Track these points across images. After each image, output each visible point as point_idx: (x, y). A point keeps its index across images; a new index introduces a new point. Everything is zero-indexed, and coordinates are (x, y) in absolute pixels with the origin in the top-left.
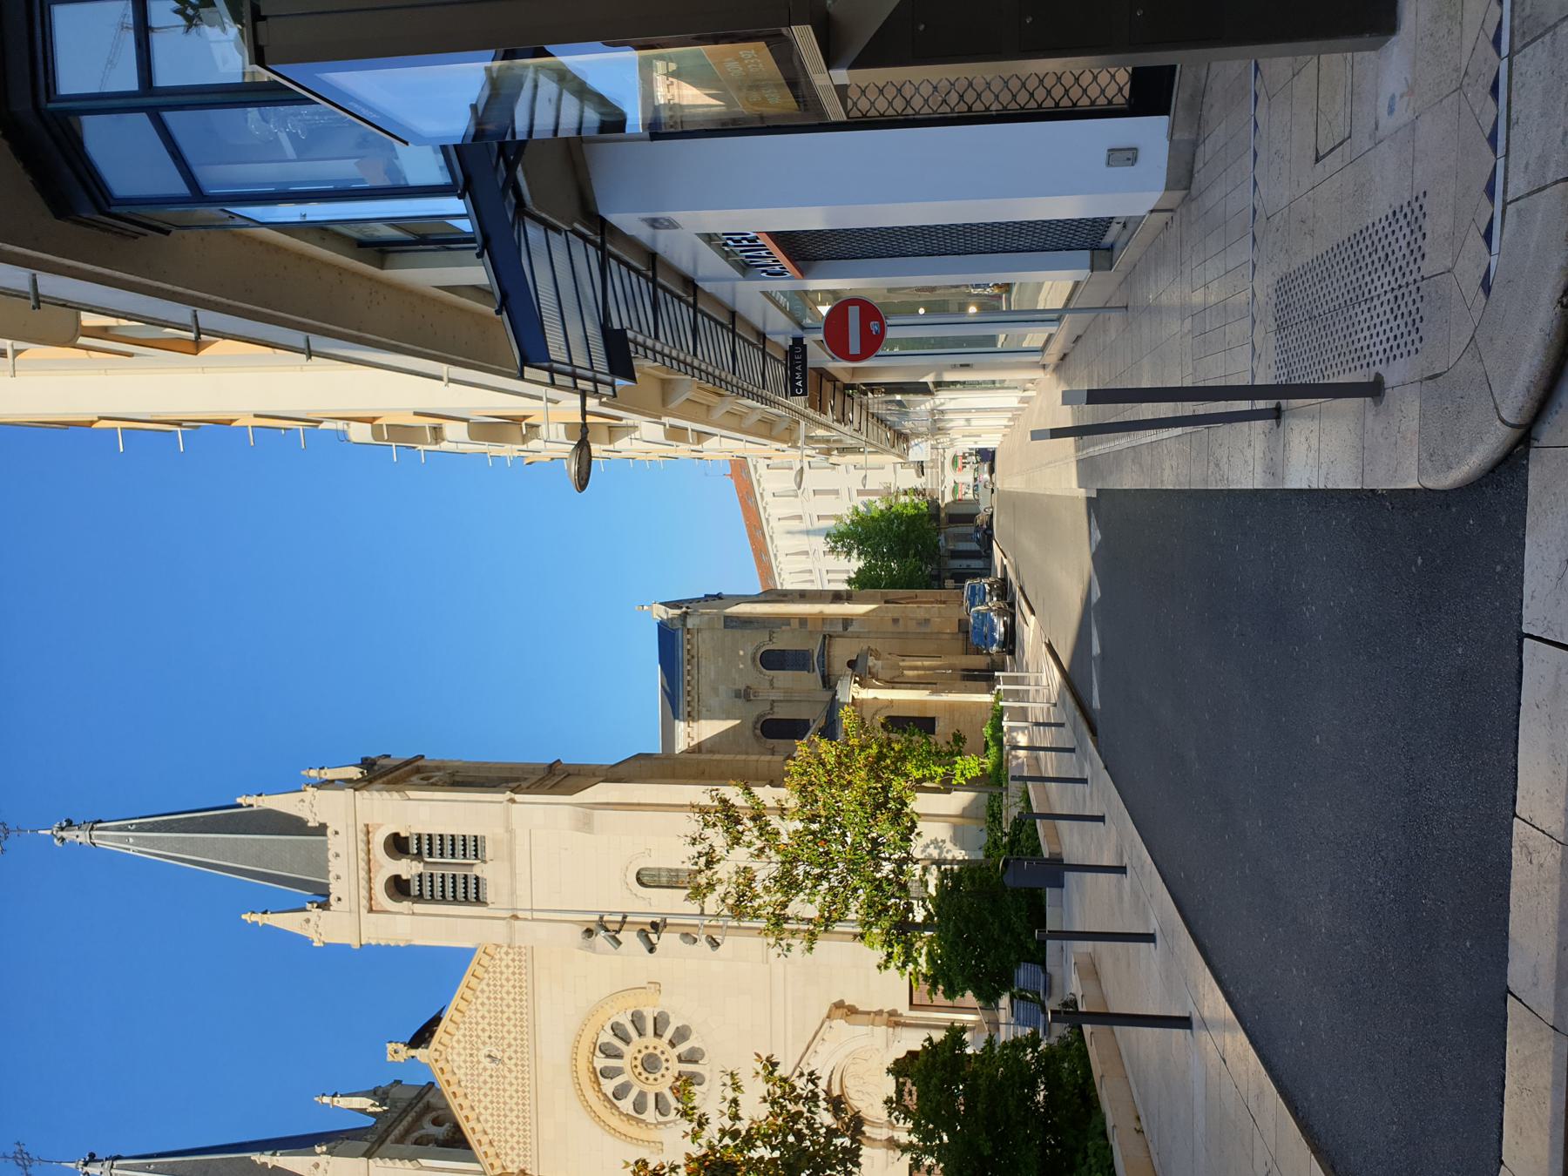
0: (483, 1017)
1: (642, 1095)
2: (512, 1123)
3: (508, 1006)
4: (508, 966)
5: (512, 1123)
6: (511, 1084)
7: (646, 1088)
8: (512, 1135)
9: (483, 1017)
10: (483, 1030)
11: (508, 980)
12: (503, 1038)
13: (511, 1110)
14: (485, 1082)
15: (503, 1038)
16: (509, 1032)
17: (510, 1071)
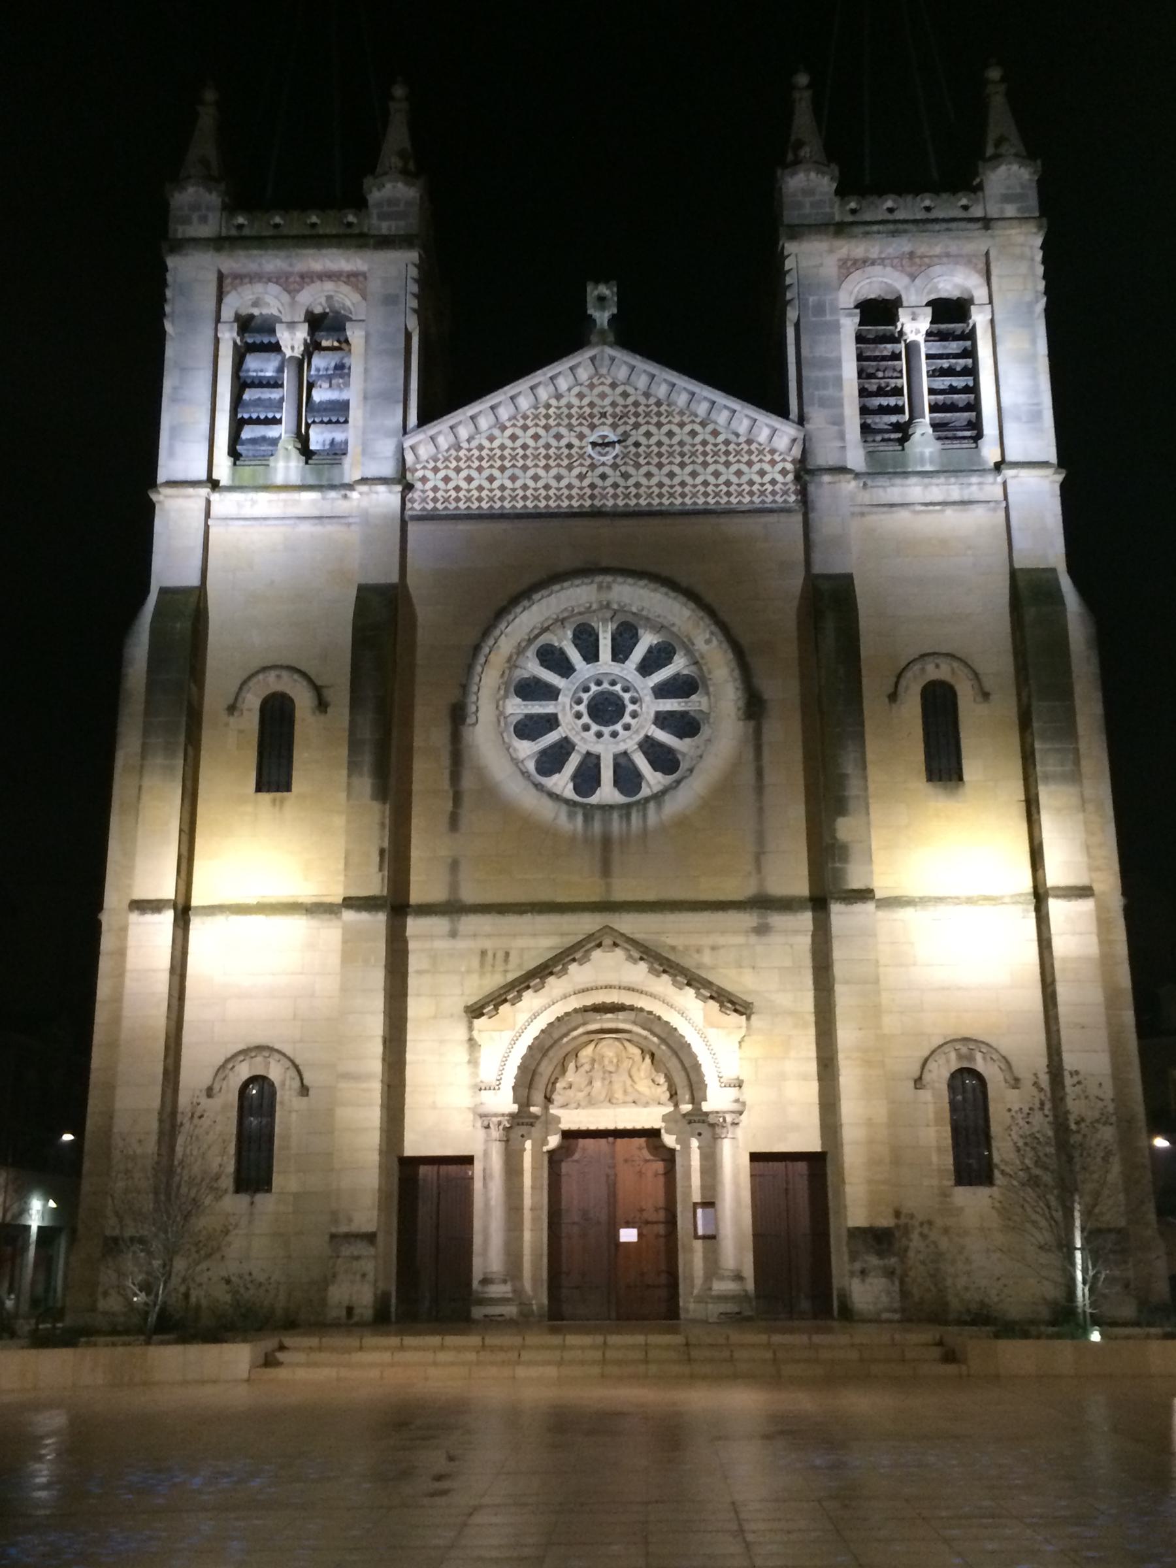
0: (670, 434)
1: (551, 693)
2: (491, 479)
3: (694, 474)
4: (762, 473)
5: (491, 479)
6: (559, 478)
7: (564, 699)
8: (469, 479)
9: (670, 434)
10: (648, 435)
11: (739, 473)
12: (637, 466)
13: (513, 478)
14: (558, 437)
15: (637, 466)
16: (649, 475)
17: (581, 477)
